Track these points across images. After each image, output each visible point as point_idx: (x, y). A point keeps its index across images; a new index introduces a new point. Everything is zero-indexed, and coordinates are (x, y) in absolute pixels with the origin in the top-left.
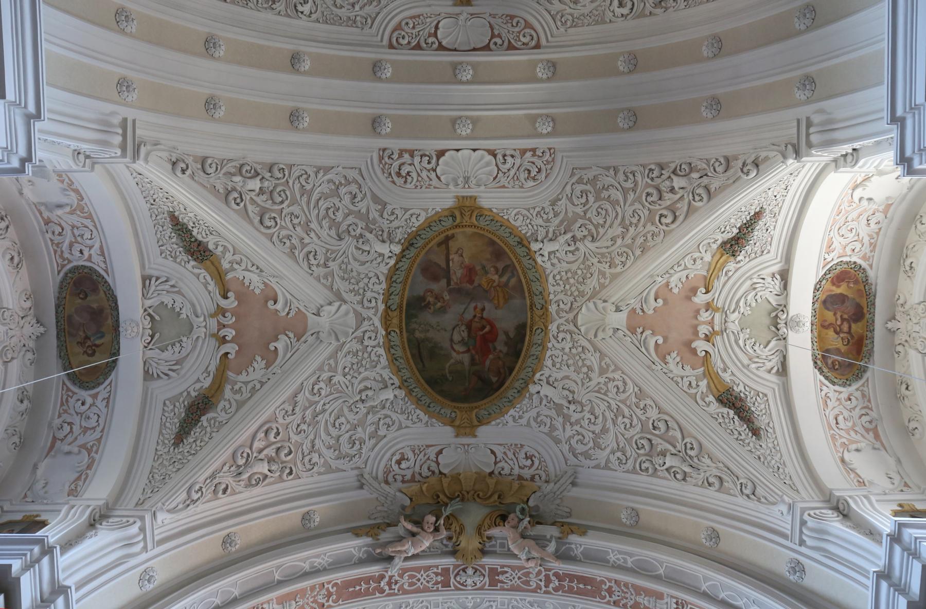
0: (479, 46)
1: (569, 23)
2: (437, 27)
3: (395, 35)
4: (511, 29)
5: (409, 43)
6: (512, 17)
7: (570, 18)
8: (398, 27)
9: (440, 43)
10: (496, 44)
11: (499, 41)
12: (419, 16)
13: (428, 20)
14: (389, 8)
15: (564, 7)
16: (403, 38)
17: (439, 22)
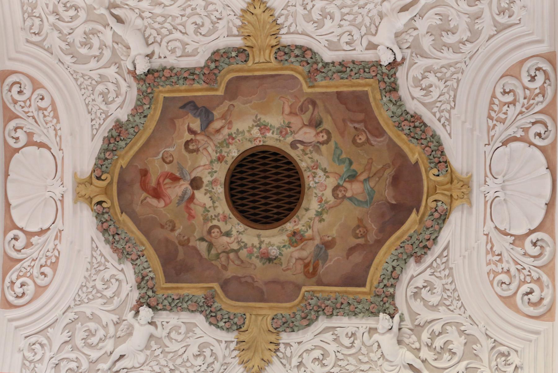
0: (14, 213)
1: (29, 355)
2: (41, 145)
3: (25, 81)
4: (37, 264)
5: (15, 102)
6: (54, 266)
7: (38, 357)
8: (36, 85)
9: (17, 150)
10: (16, 238)
11: (19, 244)
12: (56, 116)
13: (52, 133)
14: (60, 68)
15: (55, 348)
16: (20, 92)
17: (49, 149)
